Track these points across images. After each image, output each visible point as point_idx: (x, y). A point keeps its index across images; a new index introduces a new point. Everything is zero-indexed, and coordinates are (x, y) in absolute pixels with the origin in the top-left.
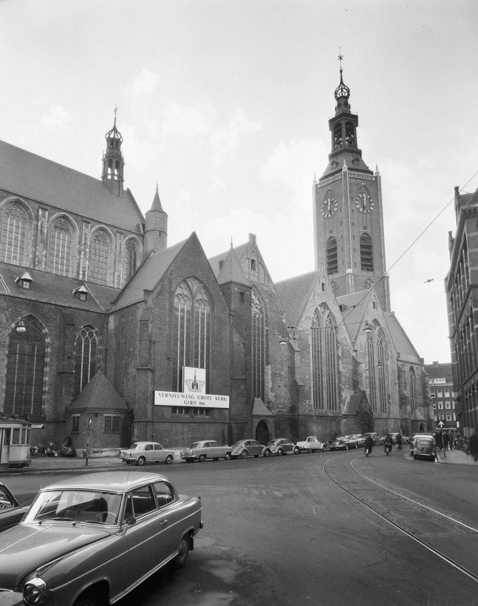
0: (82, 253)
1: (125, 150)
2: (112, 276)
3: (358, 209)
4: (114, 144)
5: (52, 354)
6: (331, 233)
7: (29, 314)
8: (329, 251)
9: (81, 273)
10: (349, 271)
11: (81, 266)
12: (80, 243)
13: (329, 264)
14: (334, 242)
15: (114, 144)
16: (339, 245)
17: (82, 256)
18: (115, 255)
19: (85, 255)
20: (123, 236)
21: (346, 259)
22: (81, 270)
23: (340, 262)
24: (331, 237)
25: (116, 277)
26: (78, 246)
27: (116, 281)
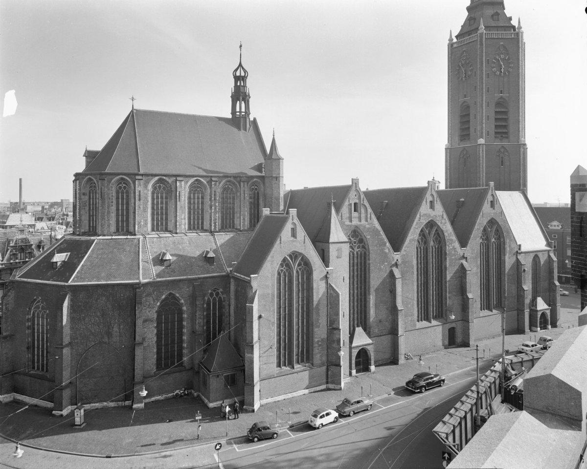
0: (213, 208)
1: (251, 86)
2: (238, 220)
3: (495, 73)
4: (240, 79)
5: (187, 318)
6: (465, 97)
7: (169, 292)
8: (462, 117)
9: (213, 225)
10: (482, 141)
11: (213, 219)
12: (211, 199)
13: (462, 130)
14: (468, 107)
15: (240, 79)
16: (472, 112)
17: (213, 211)
18: (240, 201)
19: (215, 209)
20: (246, 183)
21: (479, 128)
22: (213, 222)
23: (472, 130)
24: (465, 102)
25: (242, 221)
26: (210, 202)
27: (242, 224)
